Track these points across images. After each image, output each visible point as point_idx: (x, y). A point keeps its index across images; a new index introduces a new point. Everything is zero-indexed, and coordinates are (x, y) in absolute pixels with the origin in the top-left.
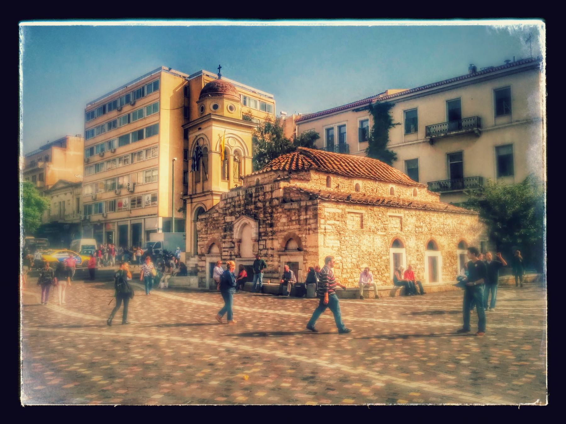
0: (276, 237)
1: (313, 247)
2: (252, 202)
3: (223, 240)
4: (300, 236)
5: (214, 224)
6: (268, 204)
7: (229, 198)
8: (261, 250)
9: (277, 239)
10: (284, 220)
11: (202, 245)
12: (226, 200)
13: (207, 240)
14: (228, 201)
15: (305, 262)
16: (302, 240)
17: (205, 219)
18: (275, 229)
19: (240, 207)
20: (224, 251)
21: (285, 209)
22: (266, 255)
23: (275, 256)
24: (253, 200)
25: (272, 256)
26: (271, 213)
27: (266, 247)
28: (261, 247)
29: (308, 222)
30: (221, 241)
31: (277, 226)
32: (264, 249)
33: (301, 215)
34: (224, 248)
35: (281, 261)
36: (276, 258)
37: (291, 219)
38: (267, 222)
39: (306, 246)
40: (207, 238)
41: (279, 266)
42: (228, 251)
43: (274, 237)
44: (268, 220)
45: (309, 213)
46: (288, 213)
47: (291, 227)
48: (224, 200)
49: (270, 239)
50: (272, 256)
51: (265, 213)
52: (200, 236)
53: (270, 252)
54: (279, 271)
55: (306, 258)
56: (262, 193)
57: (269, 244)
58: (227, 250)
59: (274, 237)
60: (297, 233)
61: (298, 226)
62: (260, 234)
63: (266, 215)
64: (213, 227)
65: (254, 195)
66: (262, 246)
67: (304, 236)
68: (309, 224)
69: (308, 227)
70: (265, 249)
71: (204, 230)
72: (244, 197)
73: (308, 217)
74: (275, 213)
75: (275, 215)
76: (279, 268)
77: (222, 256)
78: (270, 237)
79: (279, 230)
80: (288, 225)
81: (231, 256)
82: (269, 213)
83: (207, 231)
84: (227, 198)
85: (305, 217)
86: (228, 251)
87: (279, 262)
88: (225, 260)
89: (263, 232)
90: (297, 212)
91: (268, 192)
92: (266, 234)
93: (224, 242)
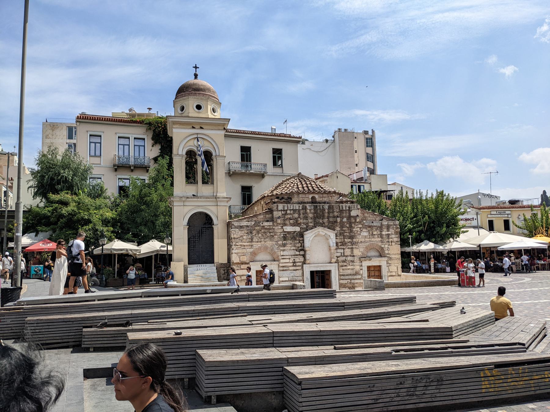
0: (357, 247)
1: (395, 254)
2: (324, 216)
3: (282, 248)
4: (382, 246)
5: (265, 233)
6: (345, 220)
7: (290, 210)
8: (338, 257)
9: (357, 248)
10: (366, 234)
11: (243, 253)
12: (287, 210)
13: (250, 248)
14: (288, 212)
16: (385, 250)
17: (247, 226)
18: (354, 240)
19: (307, 220)
22: (344, 262)
23: (355, 261)
24: (326, 215)
25: (353, 261)
28: (339, 254)
29: (390, 237)
31: (357, 238)
33: (383, 231)
34: (282, 256)
35: (363, 265)
36: (357, 263)
37: (372, 233)
38: (345, 234)
39: (388, 254)
40: (252, 246)
41: (362, 269)
42: (289, 259)
43: (354, 247)
45: (391, 230)
46: (369, 229)
47: (373, 239)
48: (281, 210)
49: (349, 248)
50: (353, 261)
52: (237, 244)
53: (349, 258)
54: (361, 273)
55: (389, 262)
59: (354, 247)
60: (380, 244)
62: (337, 244)
63: (344, 229)
64: (262, 235)
65: (326, 211)
66: (340, 253)
67: (387, 246)
68: (391, 238)
69: (390, 240)
70: (344, 256)
71: (244, 237)
72: (312, 211)
73: (390, 233)
74: (354, 228)
75: (354, 230)
76: (361, 271)
77: (279, 263)
80: (369, 238)
81: (294, 263)
83: (252, 239)
84: (286, 208)
85: (387, 233)
86: (289, 259)
87: (361, 266)
88: (283, 267)
89: (340, 242)
90: (379, 229)
92: (343, 244)
93: (284, 250)
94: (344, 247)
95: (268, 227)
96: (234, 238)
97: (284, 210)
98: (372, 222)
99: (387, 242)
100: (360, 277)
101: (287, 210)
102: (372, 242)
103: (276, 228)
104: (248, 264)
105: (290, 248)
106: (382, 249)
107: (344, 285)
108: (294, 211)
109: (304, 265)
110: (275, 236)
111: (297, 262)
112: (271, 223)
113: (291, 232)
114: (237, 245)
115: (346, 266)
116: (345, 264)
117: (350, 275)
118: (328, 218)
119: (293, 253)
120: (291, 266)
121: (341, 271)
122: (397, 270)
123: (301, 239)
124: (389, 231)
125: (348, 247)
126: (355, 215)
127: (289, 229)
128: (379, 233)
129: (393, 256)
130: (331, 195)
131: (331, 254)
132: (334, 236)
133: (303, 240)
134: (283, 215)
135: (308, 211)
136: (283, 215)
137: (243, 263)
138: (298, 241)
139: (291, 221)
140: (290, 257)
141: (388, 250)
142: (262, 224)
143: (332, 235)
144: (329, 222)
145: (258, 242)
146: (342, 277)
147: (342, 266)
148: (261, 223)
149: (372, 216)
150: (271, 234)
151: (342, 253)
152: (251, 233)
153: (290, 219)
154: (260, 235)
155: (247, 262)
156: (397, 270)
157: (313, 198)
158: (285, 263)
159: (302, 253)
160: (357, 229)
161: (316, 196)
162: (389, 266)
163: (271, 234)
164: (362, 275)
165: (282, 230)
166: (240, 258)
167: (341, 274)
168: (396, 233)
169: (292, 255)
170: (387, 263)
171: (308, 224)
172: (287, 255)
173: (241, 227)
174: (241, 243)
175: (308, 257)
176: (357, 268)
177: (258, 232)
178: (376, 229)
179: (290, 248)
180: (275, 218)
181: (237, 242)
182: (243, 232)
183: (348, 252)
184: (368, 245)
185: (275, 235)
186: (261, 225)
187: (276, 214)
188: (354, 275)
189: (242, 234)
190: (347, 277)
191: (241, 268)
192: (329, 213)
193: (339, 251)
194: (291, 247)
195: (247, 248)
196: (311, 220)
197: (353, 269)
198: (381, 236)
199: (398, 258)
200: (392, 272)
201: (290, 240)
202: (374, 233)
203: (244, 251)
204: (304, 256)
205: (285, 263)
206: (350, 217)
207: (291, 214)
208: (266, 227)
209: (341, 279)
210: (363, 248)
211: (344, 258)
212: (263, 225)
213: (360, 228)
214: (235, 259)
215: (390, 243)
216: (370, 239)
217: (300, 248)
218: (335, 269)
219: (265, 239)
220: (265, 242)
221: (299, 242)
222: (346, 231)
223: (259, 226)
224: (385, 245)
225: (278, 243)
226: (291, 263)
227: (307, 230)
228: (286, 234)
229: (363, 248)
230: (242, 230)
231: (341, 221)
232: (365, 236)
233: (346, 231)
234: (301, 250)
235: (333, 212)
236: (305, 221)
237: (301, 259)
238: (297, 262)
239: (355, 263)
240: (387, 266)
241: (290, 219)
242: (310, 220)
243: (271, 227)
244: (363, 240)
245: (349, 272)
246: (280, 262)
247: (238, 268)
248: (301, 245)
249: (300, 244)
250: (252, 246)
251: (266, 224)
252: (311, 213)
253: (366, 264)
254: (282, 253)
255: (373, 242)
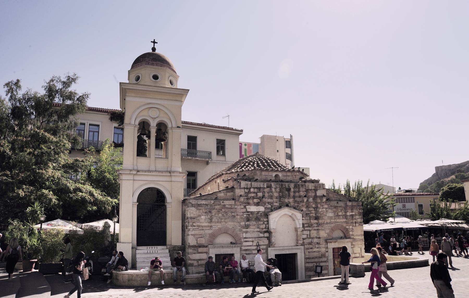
0: (323, 228)
1: (359, 235)
3: (244, 230)
4: (347, 227)
6: (311, 200)
7: (254, 188)
8: (304, 239)
9: (323, 230)
10: (331, 215)
13: (208, 229)
14: (252, 190)
15: (352, 246)
16: (349, 231)
17: (206, 204)
18: (320, 221)
20: (246, 241)
21: (331, 206)
23: (321, 243)
24: (292, 194)
26: (316, 208)
27: (310, 236)
28: (305, 236)
29: (354, 217)
30: (240, 230)
31: (323, 219)
32: (307, 238)
33: (347, 212)
34: (245, 238)
35: (329, 247)
38: (311, 215)
39: (353, 235)
42: (253, 241)
44: (311, 213)
45: (355, 211)
46: (335, 209)
47: (338, 220)
48: (244, 188)
49: (315, 230)
51: (307, 207)
52: (194, 224)
55: (354, 243)
56: (304, 190)
57: (314, 234)
58: (251, 240)
59: (320, 228)
60: (345, 225)
61: (345, 219)
63: (310, 209)
64: (223, 215)
65: (292, 190)
66: (306, 235)
67: (351, 227)
68: (355, 219)
69: (354, 221)
70: (310, 238)
72: (278, 190)
73: (354, 213)
75: (320, 210)
76: (327, 253)
77: (241, 246)
78: (316, 228)
79: (326, 222)
80: (335, 219)
82: (314, 208)
85: (351, 214)
86: (253, 241)
87: (327, 248)
88: (246, 250)
91: (311, 190)
92: (310, 225)
93: (246, 232)
94: (310, 229)
95: (230, 207)
96: (191, 218)
97: (247, 188)
98: (338, 203)
99: (351, 223)
100: (325, 259)
101: (250, 188)
102: (337, 223)
103: (239, 207)
104: (206, 247)
105: (253, 230)
106: (347, 230)
107: (310, 268)
108: (259, 189)
109: (269, 249)
110: (237, 217)
111: (261, 245)
112: (233, 202)
113: (255, 212)
114: (194, 226)
115: (311, 248)
116: (311, 246)
117: (316, 257)
118: (294, 197)
119: (255, 235)
120: (254, 250)
121: (307, 254)
122: (361, 251)
123: (265, 220)
124: (352, 212)
125: (314, 228)
126: (321, 195)
127: (253, 209)
128: (344, 214)
129: (357, 237)
130: (295, 174)
131: (297, 235)
132: (301, 216)
133: (268, 221)
134: (246, 193)
135: (273, 190)
136: (246, 193)
137: (200, 246)
138: (262, 223)
139: (255, 201)
140: (254, 239)
141: (352, 231)
142: (223, 202)
143: (299, 215)
144: (295, 201)
145: (218, 222)
146: (308, 261)
147: (308, 249)
148: (221, 202)
149: (336, 196)
150: (233, 214)
151: (308, 235)
152: (210, 212)
153: (253, 198)
154: (220, 215)
155: (205, 245)
156: (361, 251)
157: (276, 176)
158: (248, 246)
159: (267, 235)
160: (323, 210)
161: (280, 175)
162: (353, 247)
163: (233, 214)
164: (327, 257)
165: (245, 209)
166: (197, 240)
167: (307, 257)
168: (360, 214)
169: (255, 238)
170: (352, 245)
171: (273, 203)
172: (250, 238)
173: (199, 205)
174: (199, 224)
175: (273, 239)
176: (323, 250)
177: (219, 211)
178: (341, 210)
179: (253, 230)
180: (238, 196)
181: (194, 223)
182: (201, 211)
183: (314, 234)
184: (334, 226)
185: (237, 215)
186: (222, 204)
187: (238, 192)
188: (320, 257)
189: (200, 214)
190: (313, 260)
191: (198, 251)
192: (294, 192)
193: (305, 232)
194: (254, 229)
195: (206, 230)
196: (276, 199)
197: (319, 252)
198: (345, 217)
199: (361, 239)
200: (356, 253)
201: (254, 221)
202: (340, 214)
203: (202, 232)
204: (269, 238)
205: (248, 246)
206: (315, 197)
207: (254, 193)
208: (227, 206)
209: (308, 263)
210: (329, 229)
211: (310, 240)
212: (223, 204)
213: (326, 208)
214: (191, 241)
215: (354, 224)
216: (336, 220)
217: (264, 230)
218: (301, 252)
219: (226, 219)
220: (226, 222)
221: (264, 223)
222: (312, 212)
223: (219, 205)
224: (349, 226)
225: (240, 224)
226: (254, 246)
227: (272, 211)
228: (248, 215)
229: (329, 229)
230: (200, 209)
231: (307, 201)
232: (331, 217)
233: (312, 212)
234: (265, 232)
235: (299, 192)
236: (270, 200)
237: (265, 241)
238: (261, 245)
239: (321, 245)
240: (352, 248)
241: (253, 198)
242: (275, 200)
243: (233, 206)
244: (328, 221)
245: (315, 254)
246: (242, 245)
247: (195, 252)
248: (266, 226)
249: (264, 226)
250: (211, 226)
251: (226, 203)
252: (276, 192)
253: (332, 245)
254: (244, 235)
255: (339, 223)
